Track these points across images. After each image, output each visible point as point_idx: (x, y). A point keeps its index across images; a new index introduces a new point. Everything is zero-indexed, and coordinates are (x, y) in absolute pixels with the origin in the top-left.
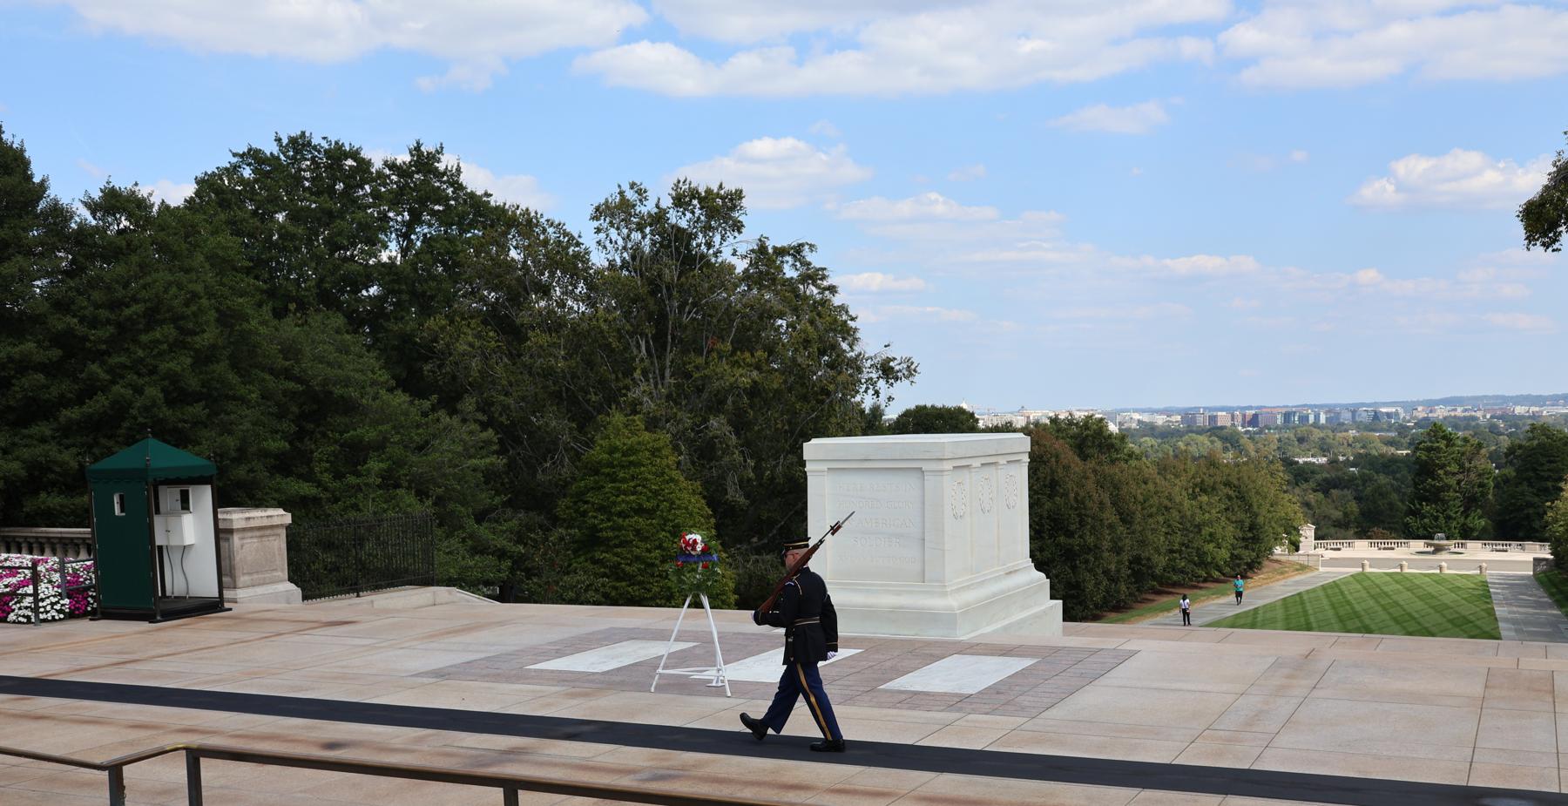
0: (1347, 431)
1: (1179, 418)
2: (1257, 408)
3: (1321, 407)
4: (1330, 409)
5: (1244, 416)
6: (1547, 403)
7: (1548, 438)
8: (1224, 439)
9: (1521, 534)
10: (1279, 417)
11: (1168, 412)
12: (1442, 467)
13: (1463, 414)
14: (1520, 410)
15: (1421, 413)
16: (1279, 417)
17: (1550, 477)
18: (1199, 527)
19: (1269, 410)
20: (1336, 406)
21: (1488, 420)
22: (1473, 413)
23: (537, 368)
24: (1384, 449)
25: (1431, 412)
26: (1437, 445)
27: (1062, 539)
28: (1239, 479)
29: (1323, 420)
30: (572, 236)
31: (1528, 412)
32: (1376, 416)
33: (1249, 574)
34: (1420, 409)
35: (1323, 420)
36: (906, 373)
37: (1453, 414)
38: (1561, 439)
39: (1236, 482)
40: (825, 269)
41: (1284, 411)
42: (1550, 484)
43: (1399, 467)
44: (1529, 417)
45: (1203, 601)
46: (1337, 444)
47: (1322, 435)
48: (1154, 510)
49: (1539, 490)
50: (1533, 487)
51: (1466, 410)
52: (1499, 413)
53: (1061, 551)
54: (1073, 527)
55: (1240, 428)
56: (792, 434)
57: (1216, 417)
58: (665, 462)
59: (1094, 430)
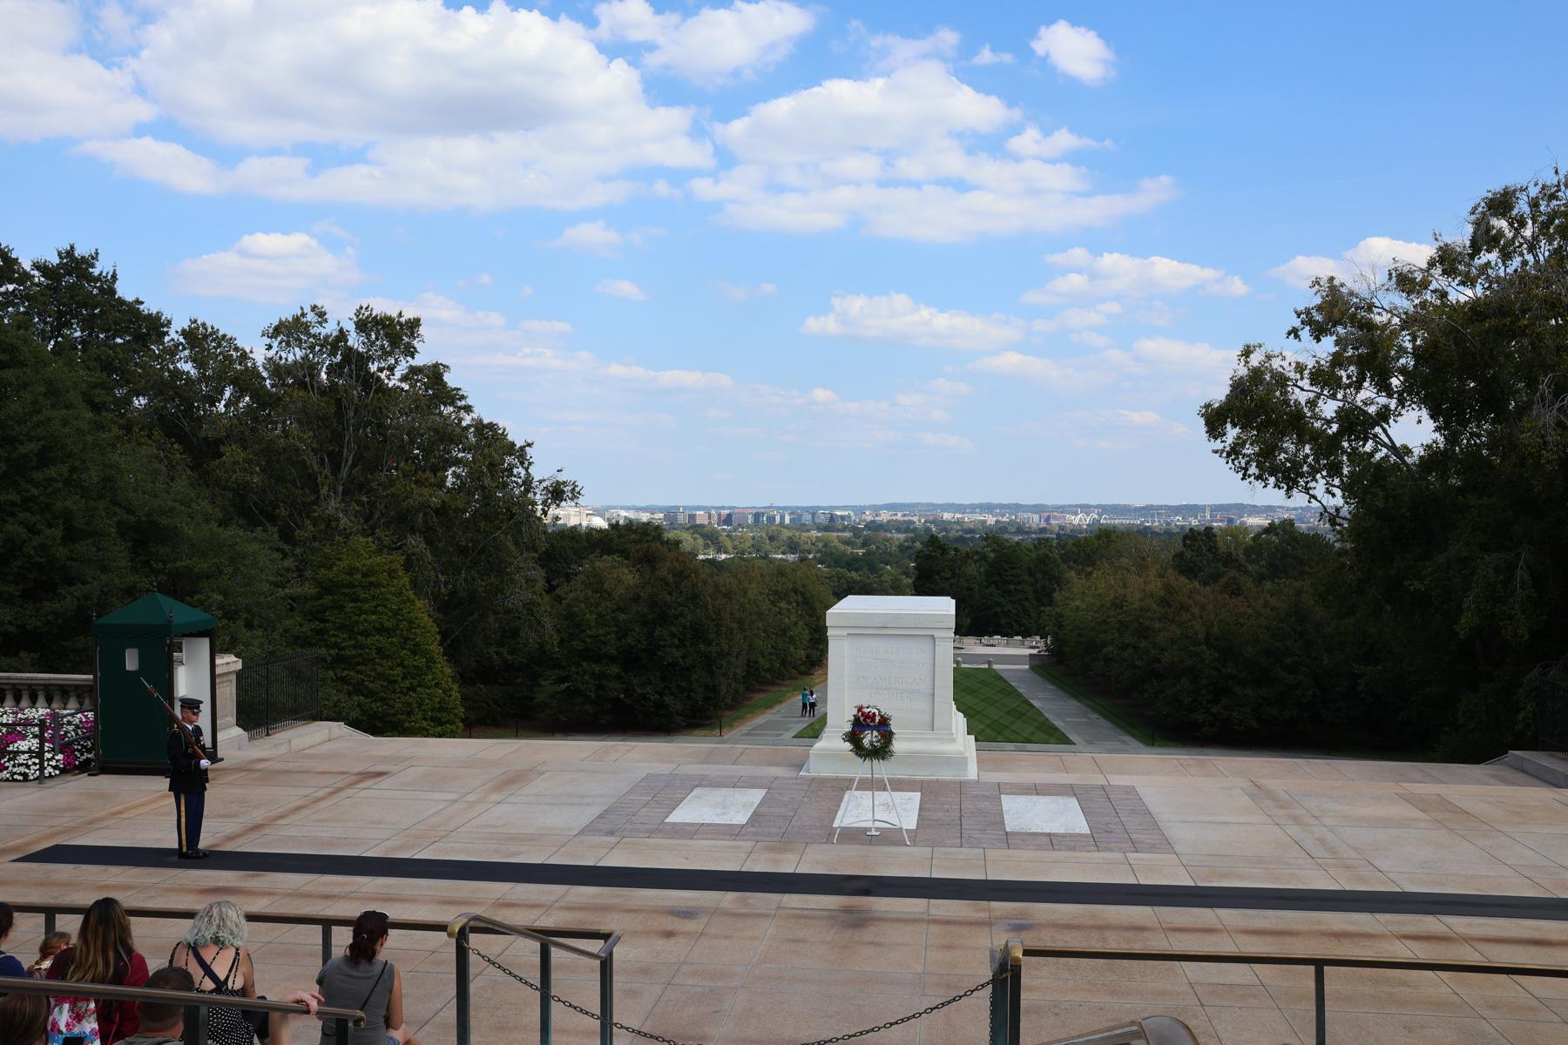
0: (808, 531)
1: (661, 516)
2: (729, 508)
3: (785, 508)
4: (793, 511)
5: (719, 515)
6: (968, 511)
7: (998, 545)
8: (705, 536)
9: (990, 629)
10: (750, 517)
11: (652, 510)
12: (938, 573)
13: (903, 519)
14: (947, 516)
15: (868, 517)
16: (750, 517)
17: (1012, 581)
18: (784, 631)
19: (741, 510)
20: (799, 508)
21: (923, 524)
22: (911, 518)
23: (233, 483)
24: (842, 547)
25: (877, 516)
26: (934, 554)
27: (702, 646)
28: (804, 586)
29: (787, 521)
30: (245, 352)
31: (953, 518)
32: (832, 518)
33: (812, 671)
34: (868, 513)
35: (787, 521)
36: (570, 495)
37: (894, 518)
38: (1009, 547)
39: (801, 589)
40: (460, 389)
41: (754, 512)
42: (1012, 587)
43: (861, 565)
44: (955, 522)
45: (790, 698)
46: (802, 543)
47: (790, 534)
48: (754, 617)
49: (1003, 592)
50: (999, 589)
51: (904, 515)
52: (931, 518)
53: (701, 658)
54: (711, 636)
55: (716, 526)
56: (473, 551)
57: (695, 515)
58: (402, 582)
59: (654, 537)
